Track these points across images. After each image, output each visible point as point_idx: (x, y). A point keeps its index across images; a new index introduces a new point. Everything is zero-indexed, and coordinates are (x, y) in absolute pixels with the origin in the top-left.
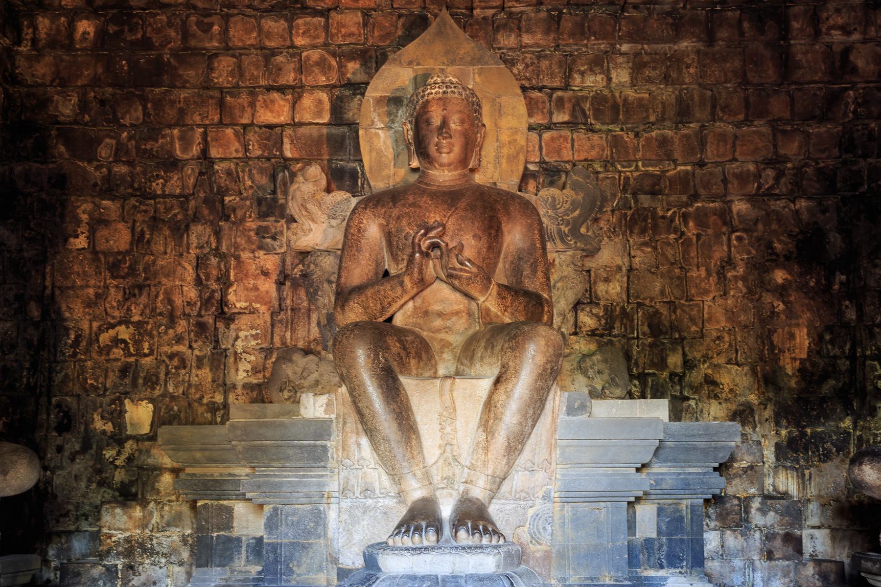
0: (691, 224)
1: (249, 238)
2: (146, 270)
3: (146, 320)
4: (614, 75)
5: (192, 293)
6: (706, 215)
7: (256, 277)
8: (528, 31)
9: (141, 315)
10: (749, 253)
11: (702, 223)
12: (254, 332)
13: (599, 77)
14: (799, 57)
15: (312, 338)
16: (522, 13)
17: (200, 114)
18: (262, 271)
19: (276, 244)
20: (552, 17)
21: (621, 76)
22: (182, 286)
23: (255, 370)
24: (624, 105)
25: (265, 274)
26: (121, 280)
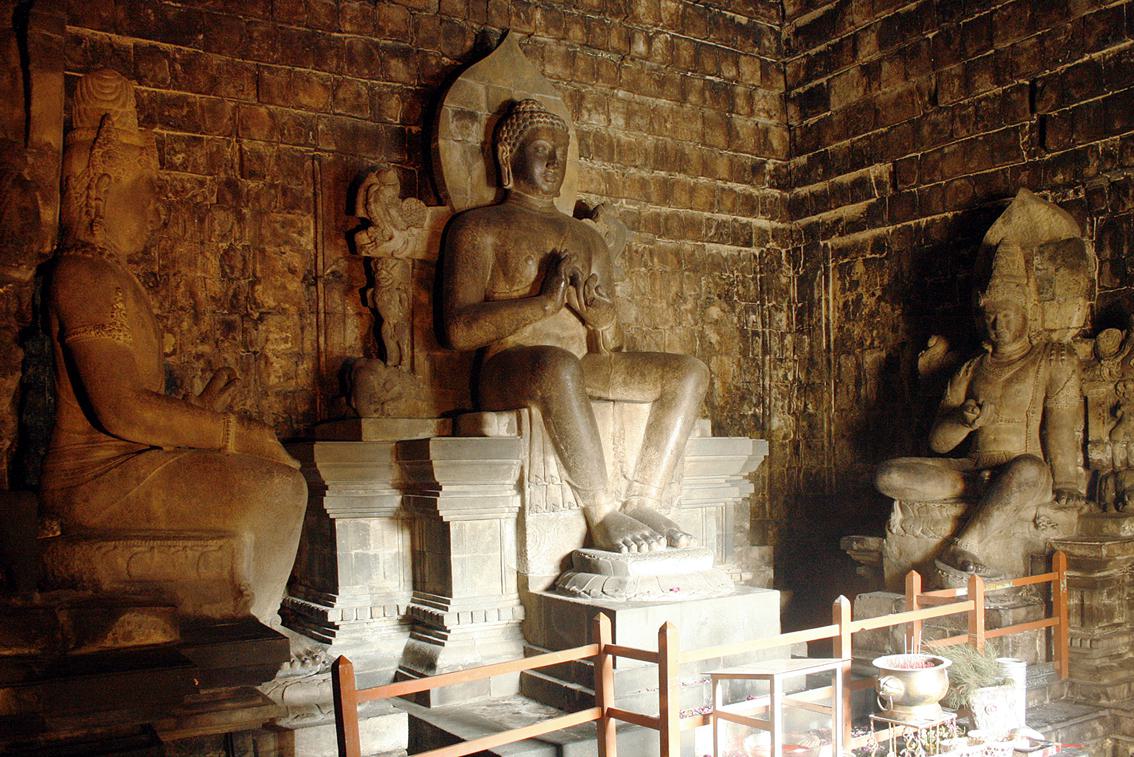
0: (656, 260)
1: (274, 230)
2: (164, 255)
3: (165, 314)
4: (612, 116)
5: (216, 287)
6: (666, 255)
7: (283, 275)
8: (549, 62)
9: (160, 308)
10: (695, 291)
11: (663, 261)
12: (284, 335)
13: (603, 117)
15: (347, 345)
16: (545, 43)
17: (235, 87)
18: (289, 269)
19: (303, 240)
20: (568, 52)
21: (619, 120)
22: (205, 278)
23: (287, 377)
24: (617, 146)
25: (293, 271)
26: (135, 266)
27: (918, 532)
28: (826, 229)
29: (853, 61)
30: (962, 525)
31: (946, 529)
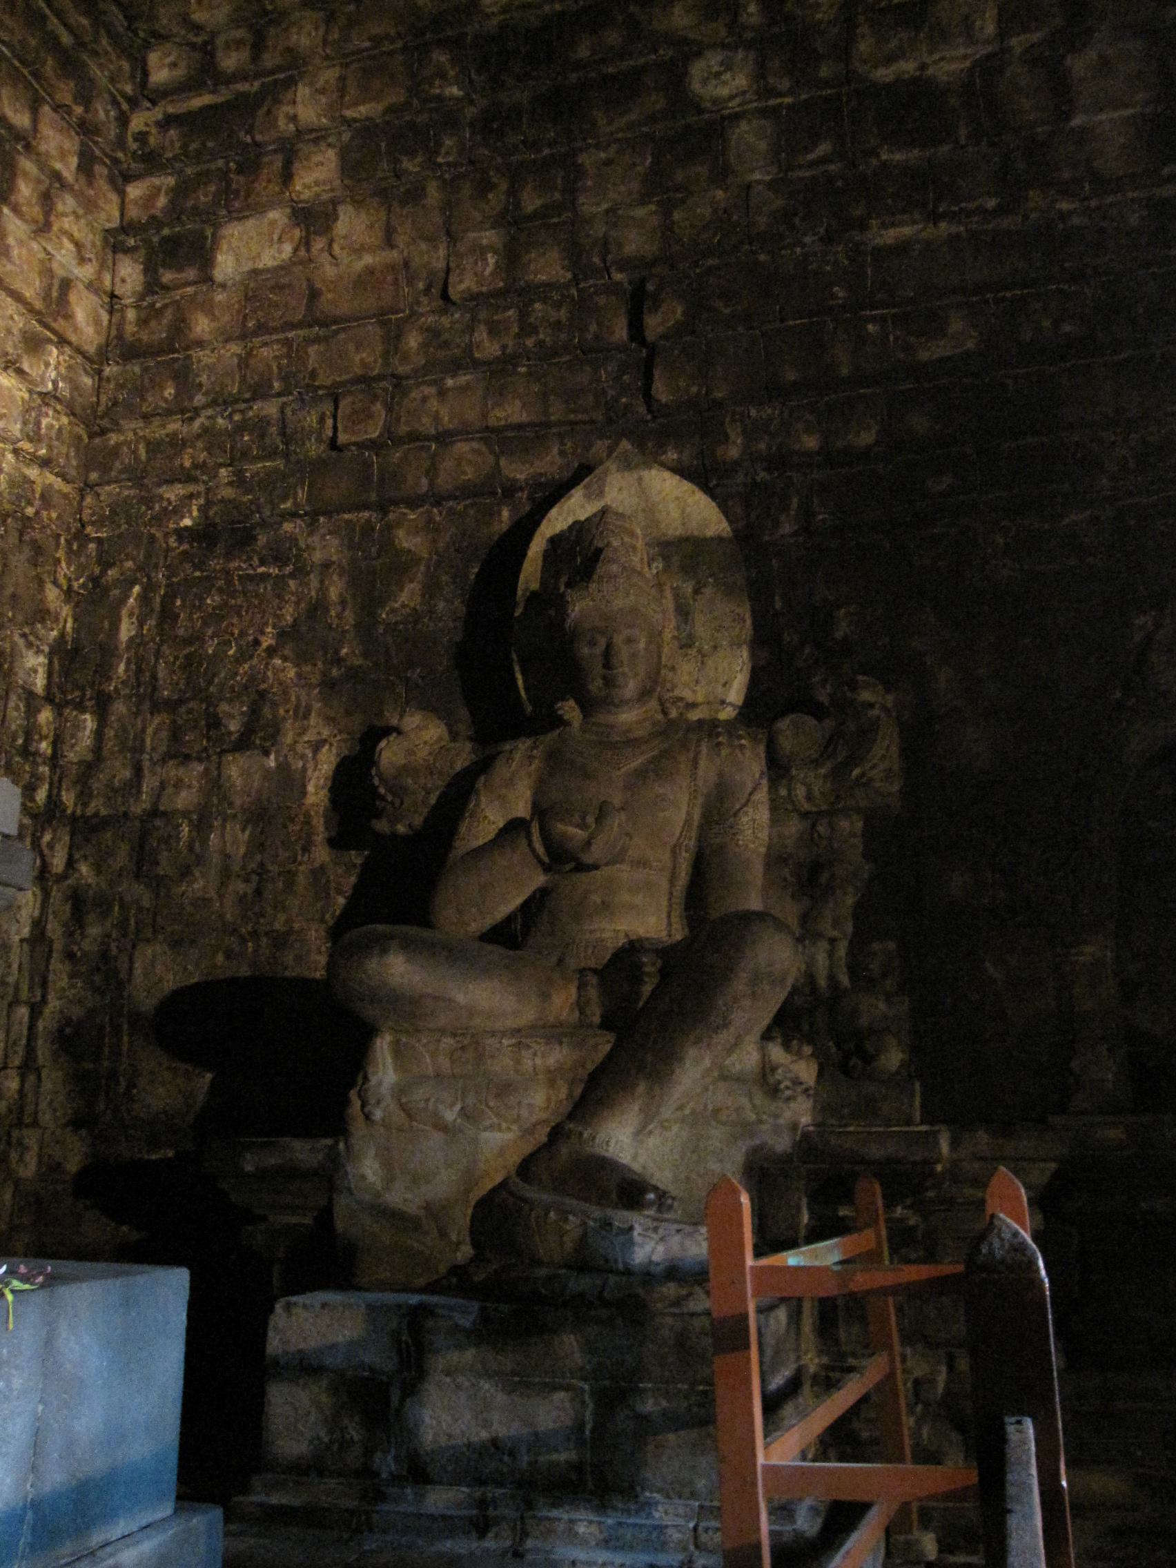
14: (11, 241)
27: (450, 1116)
28: (165, 509)
29: (282, 192)
30: (594, 1094)
31: (539, 1103)
